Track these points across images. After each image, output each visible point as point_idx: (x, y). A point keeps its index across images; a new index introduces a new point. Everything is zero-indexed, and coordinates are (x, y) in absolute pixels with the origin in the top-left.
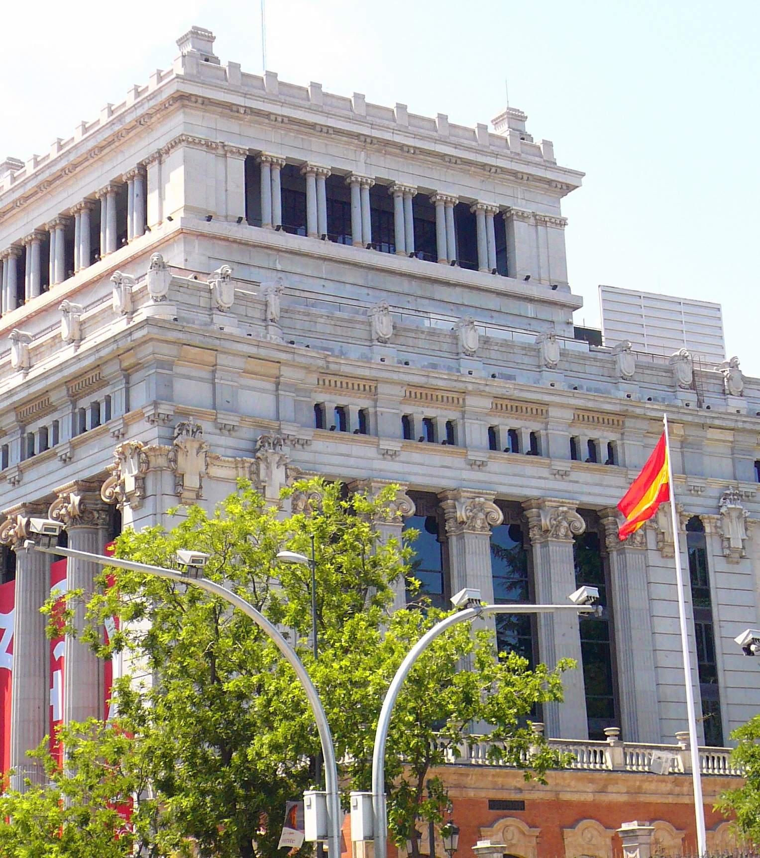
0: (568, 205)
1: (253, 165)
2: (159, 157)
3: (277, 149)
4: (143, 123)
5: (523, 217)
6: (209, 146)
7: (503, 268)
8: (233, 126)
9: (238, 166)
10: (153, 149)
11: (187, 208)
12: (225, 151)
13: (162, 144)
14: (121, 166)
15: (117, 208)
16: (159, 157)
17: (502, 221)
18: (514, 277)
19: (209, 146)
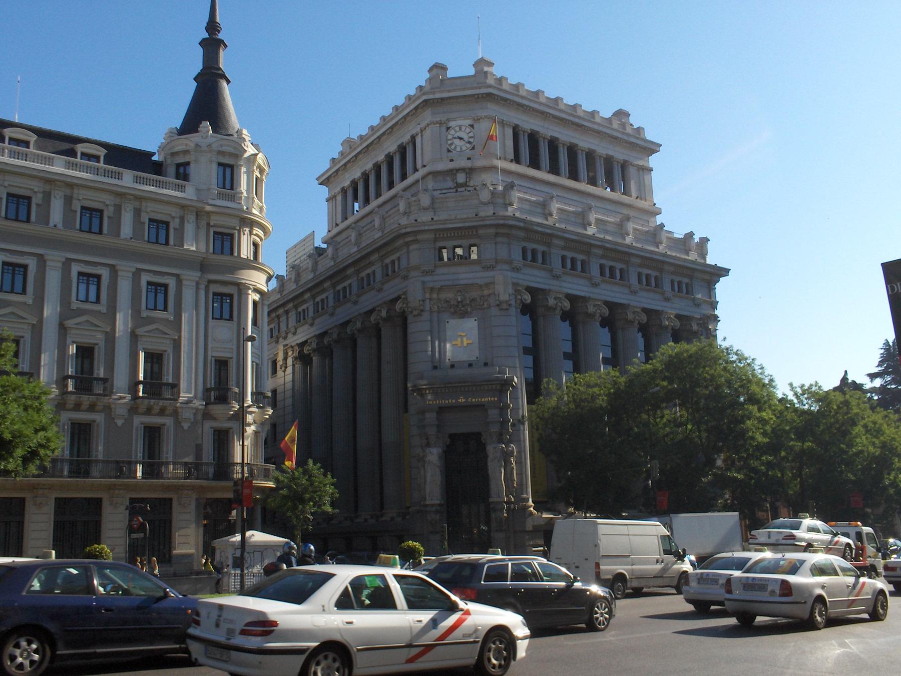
0: (653, 161)
1: (516, 132)
3: (529, 123)
9: (509, 132)
12: (502, 123)
17: (624, 166)
18: (631, 196)
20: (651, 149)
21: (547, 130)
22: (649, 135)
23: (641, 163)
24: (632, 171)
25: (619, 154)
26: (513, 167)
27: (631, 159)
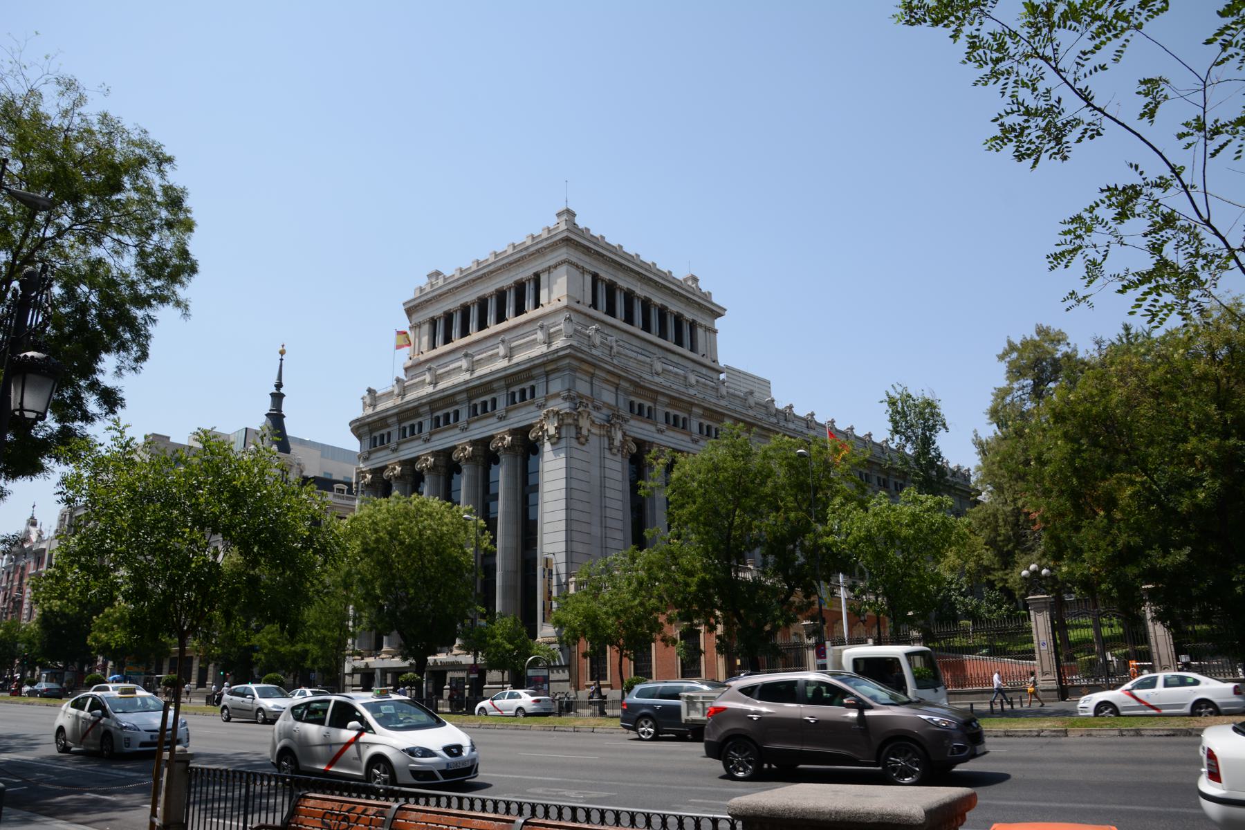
0: (719, 324)
1: (595, 278)
2: (549, 270)
3: (606, 274)
4: (540, 252)
5: (701, 326)
6: (577, 266)
7: (693, 349)
8: (587, 259)
9: (589, 279)
10: (546, 265)
11: (568, 296)
12: (584, 271)
13: (552, 263)
14: (525, 273)
15: (522, 294)
16: (549, 270)
17: (693, 325)
19: (577, 266)
20: (716, 313)
21: (624, 282)
22: (716, 299)
23: (708, 325)
24: (700, 331)
25: (689, 314)
26: (592, 312)
27: (699, 321)
